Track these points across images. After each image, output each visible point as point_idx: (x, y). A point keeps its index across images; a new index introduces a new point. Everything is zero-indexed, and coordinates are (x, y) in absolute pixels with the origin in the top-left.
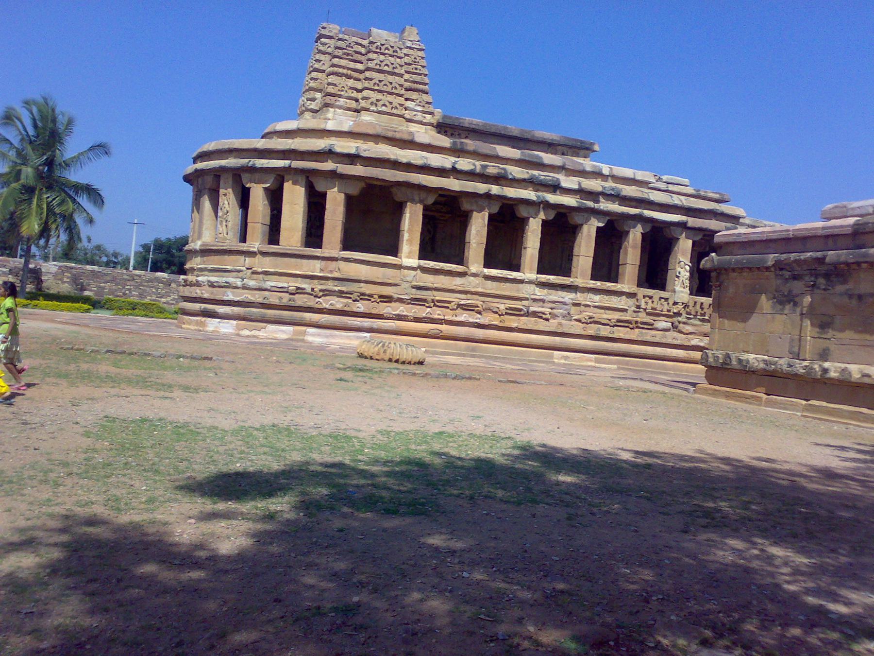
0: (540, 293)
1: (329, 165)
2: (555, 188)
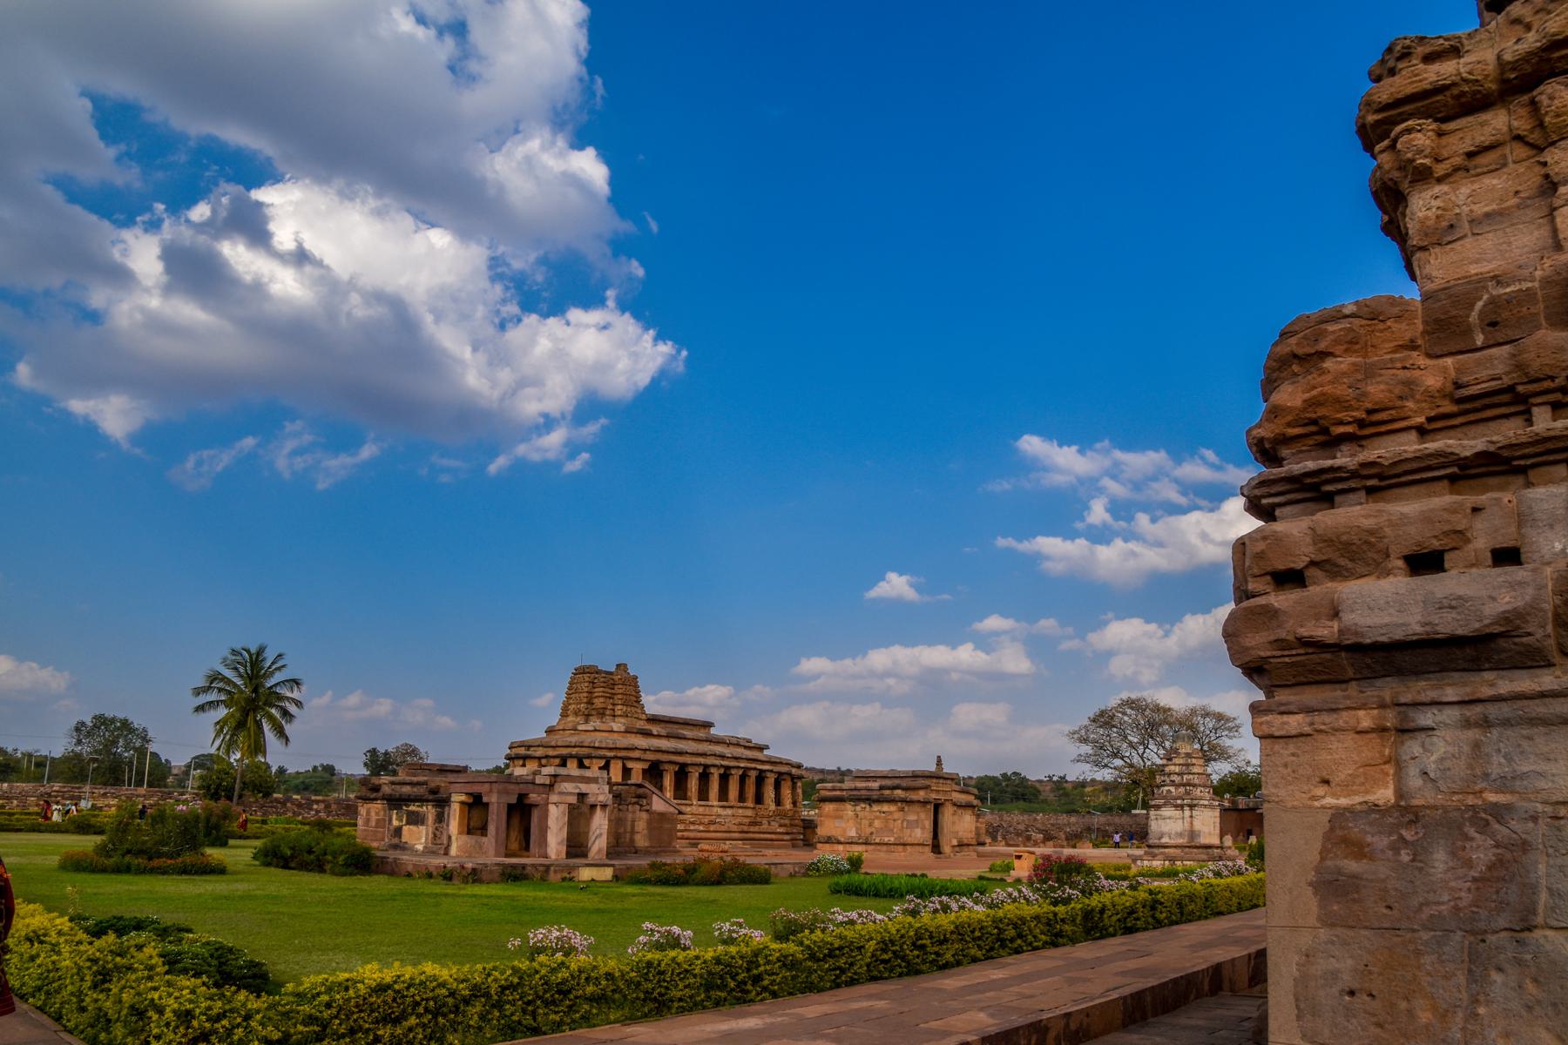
0: (720, 811)
1: (636, 754)
2: (723, 757)
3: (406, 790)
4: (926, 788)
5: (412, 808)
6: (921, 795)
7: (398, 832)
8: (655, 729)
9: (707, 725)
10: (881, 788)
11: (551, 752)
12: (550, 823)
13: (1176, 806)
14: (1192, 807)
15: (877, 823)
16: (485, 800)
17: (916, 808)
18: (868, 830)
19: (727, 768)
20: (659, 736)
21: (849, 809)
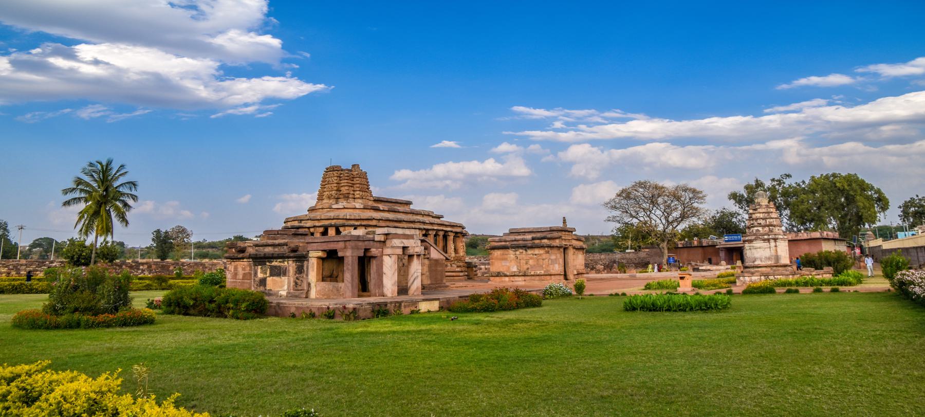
2: (424, 223)
3: (268, 250)
4: (560, 238)
5: (275, 263)
6: (557, 243)
7: (263, 282)
8: (381, 206)
9: (408, 203)
10: (533, 239)
11: (317, 224)
12: (385, 269)
13: (764, 240)
14: (775, 240)
15: (531, 262)
16: (340, 254)
17: (555, 251)
18: (526, 267)
19: (427, 230)
20: (383, 211)
21: (511, 253)
